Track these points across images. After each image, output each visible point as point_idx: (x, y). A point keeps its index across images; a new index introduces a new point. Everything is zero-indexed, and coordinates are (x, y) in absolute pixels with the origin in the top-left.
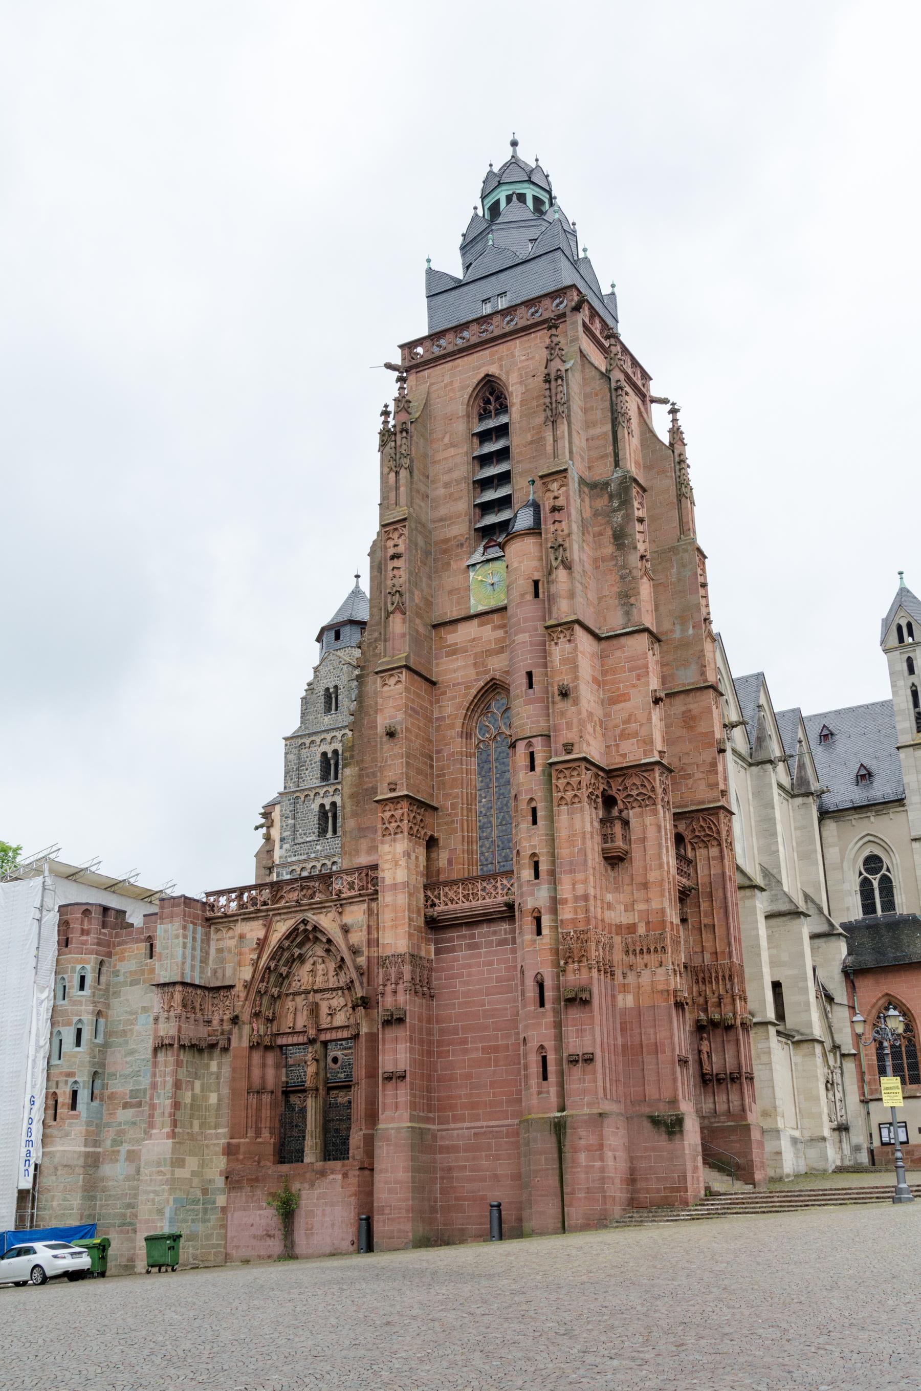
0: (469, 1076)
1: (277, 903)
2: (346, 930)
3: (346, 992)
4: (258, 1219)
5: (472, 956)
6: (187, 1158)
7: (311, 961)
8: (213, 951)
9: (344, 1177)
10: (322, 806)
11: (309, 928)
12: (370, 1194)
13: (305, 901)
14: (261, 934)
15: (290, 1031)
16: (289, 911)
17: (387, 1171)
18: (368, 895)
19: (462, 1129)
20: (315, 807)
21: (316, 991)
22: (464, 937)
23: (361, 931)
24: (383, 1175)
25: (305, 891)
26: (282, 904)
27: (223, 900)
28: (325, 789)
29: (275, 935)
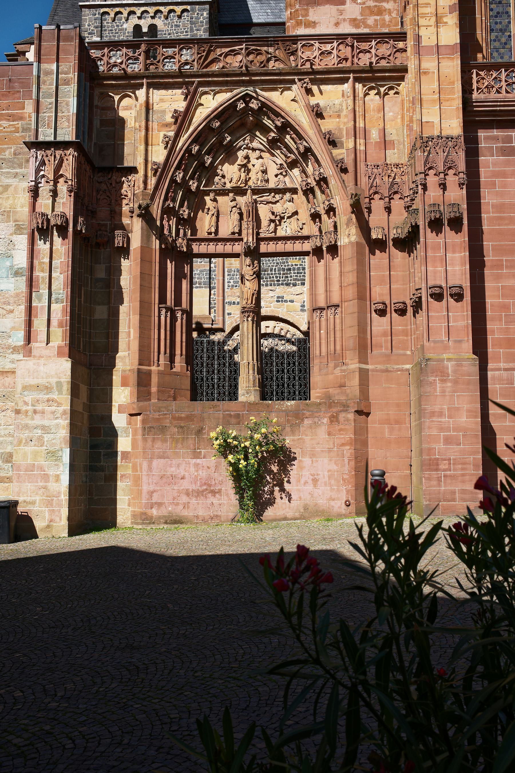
0: (505, 307)
1: (206, 67)
2: (318, 114)
3: (300, 198)
4: (192, 469)
5: (507, 163)
6: (81, 385)
7: (241, 154)
8: (97, 123)
9: (331, 422)
10: (137, 28)
11: (254, 105)
12: (365, 444)
13: (253, 68)
14: (181, 105)
15: (211, 237)
16: (225, 80)
17: (441, 414)
18: (354, 72)
19: (499, 369)
20: (129, 26)
21: (256, 191)
22: (496, 139)
23: (339, 116)
24: (435, 419)
25: (251, 57)
26: (216, 67)
27: (117, 57)
28: (143, 9)
29: (198, 111)
